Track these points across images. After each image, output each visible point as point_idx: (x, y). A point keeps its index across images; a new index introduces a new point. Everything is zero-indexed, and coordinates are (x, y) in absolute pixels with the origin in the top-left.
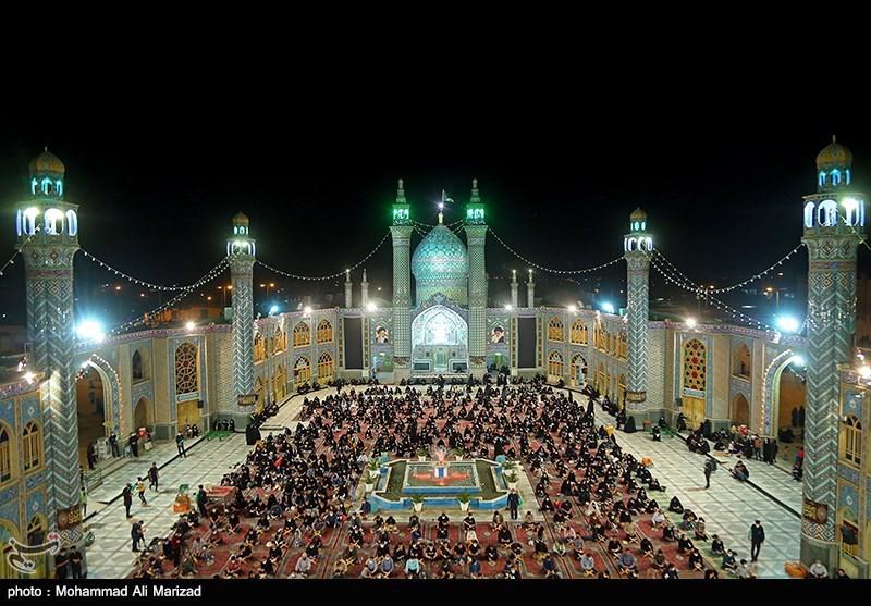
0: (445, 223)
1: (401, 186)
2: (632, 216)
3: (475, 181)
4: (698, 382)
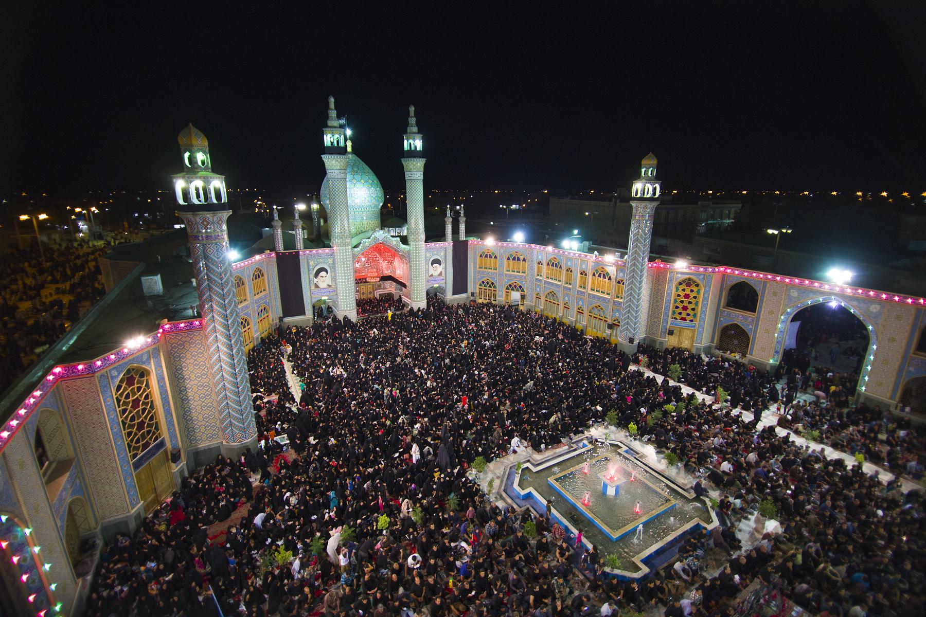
1: (332, 105)
2: (644, 162)
3: (412, 109)
4: (688, 315)
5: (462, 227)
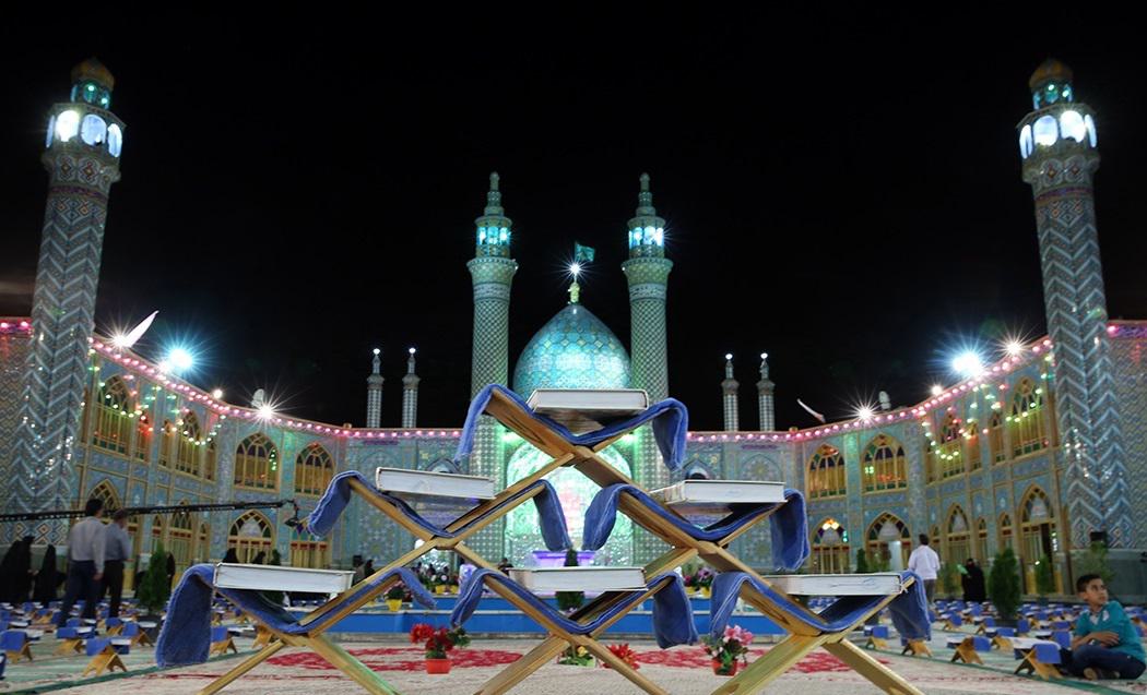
0: (584, 299)
1: (495, 184)
3: (645, 178)
5: (766, 403)
